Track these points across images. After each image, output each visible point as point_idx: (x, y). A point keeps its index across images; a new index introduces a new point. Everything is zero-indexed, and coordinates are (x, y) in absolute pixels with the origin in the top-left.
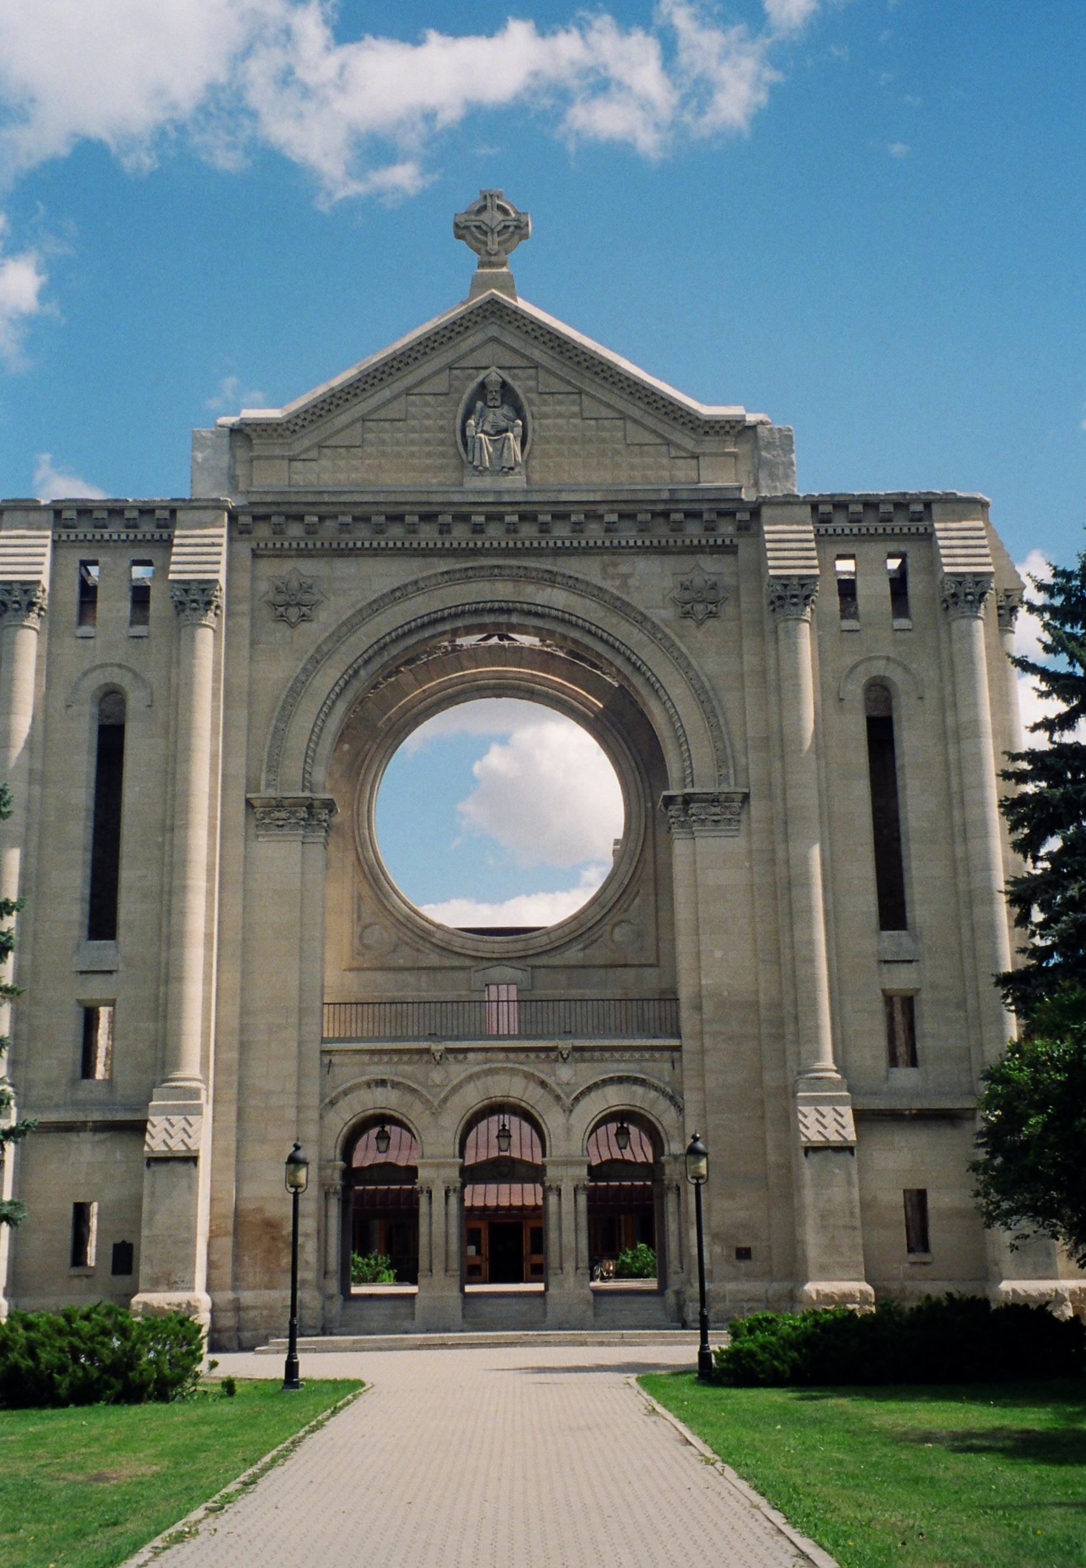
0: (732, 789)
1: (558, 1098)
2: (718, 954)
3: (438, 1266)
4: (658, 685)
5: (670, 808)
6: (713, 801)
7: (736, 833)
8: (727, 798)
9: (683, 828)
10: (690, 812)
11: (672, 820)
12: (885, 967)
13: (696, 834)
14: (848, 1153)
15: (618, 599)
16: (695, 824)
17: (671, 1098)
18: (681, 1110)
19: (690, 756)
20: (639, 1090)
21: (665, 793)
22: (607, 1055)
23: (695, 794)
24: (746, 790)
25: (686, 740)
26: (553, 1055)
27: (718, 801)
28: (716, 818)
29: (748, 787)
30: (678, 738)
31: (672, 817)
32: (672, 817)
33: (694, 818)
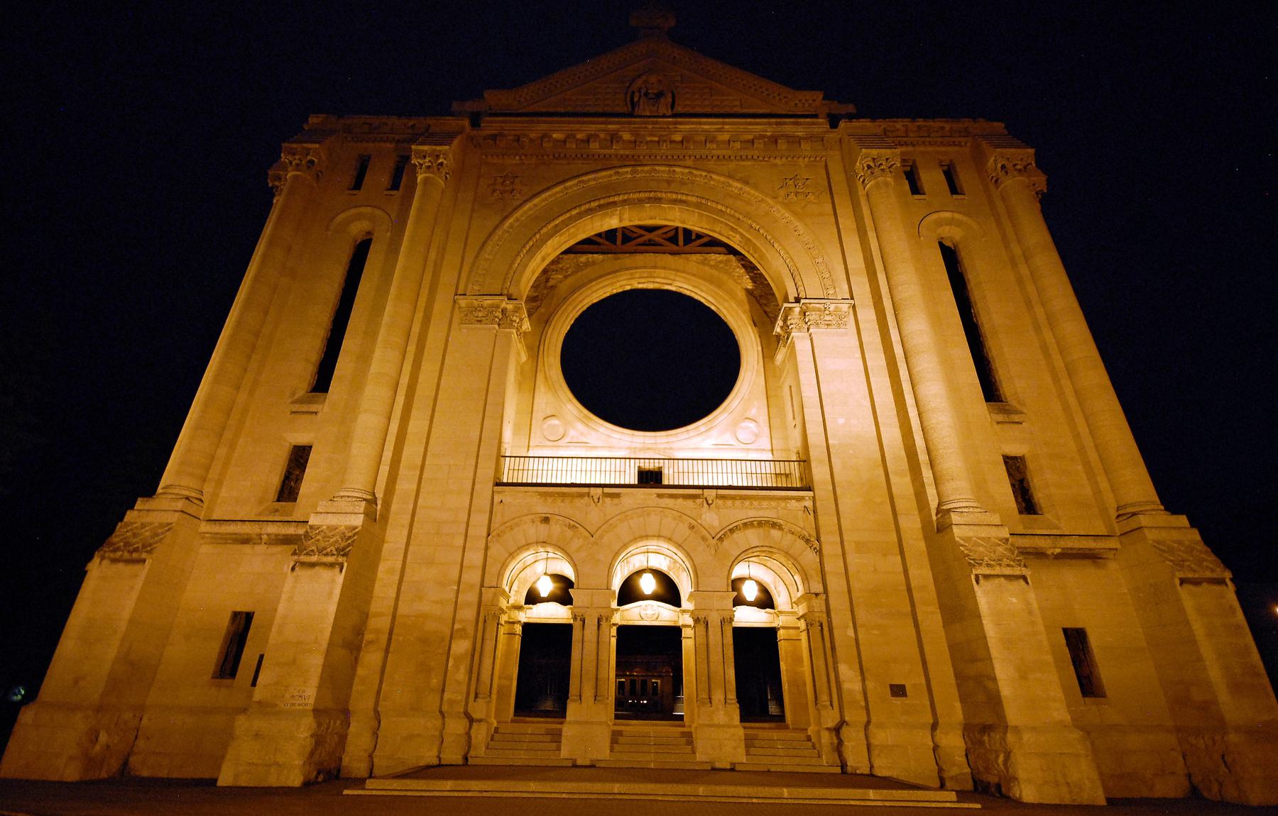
1: (704, 539)
2: (841, 421)
3: (588, 693)
8: (836, 307)
12: (1000, 425)
14: (1022, 582)
17: (807, 541)
18: (820, 552)
20: (775, 533)
22: (747, 503)
26: (699, 501)
28: (829, 323)
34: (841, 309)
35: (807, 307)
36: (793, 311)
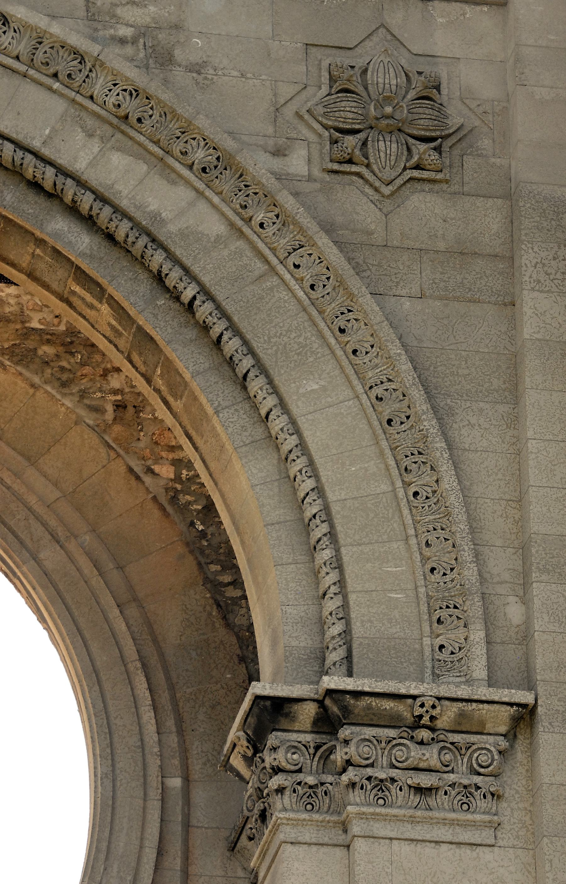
0: (484, 692)
4: (247, 363)
5: (273, 739)
6: (417, 723)
7: (486, 836)
8: (462, 715)
9: (311, 807)
10: (339, 757)
11: (276, 781)
13: (356, 828)
15: (135, 93)
16: (356, 796)
19: (341, 583)
21: (257, 688)
23: (358, 694)
24: (527, 698)
25: (332, 535)
27: (433, 729)
28: (425, 780)
29: (531, 686)
30: (307, 528)
31: (277, 770)
32: (277, 770)
33: (351, 774)
34: (482, 723)
35: (346, 710)
36: (291, 717)
